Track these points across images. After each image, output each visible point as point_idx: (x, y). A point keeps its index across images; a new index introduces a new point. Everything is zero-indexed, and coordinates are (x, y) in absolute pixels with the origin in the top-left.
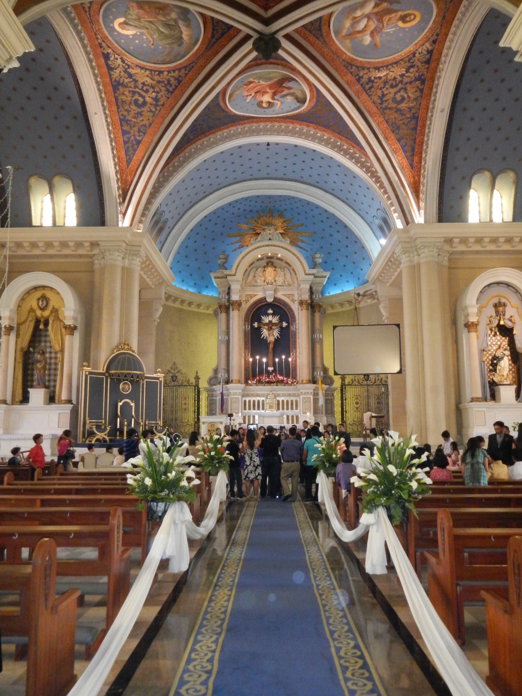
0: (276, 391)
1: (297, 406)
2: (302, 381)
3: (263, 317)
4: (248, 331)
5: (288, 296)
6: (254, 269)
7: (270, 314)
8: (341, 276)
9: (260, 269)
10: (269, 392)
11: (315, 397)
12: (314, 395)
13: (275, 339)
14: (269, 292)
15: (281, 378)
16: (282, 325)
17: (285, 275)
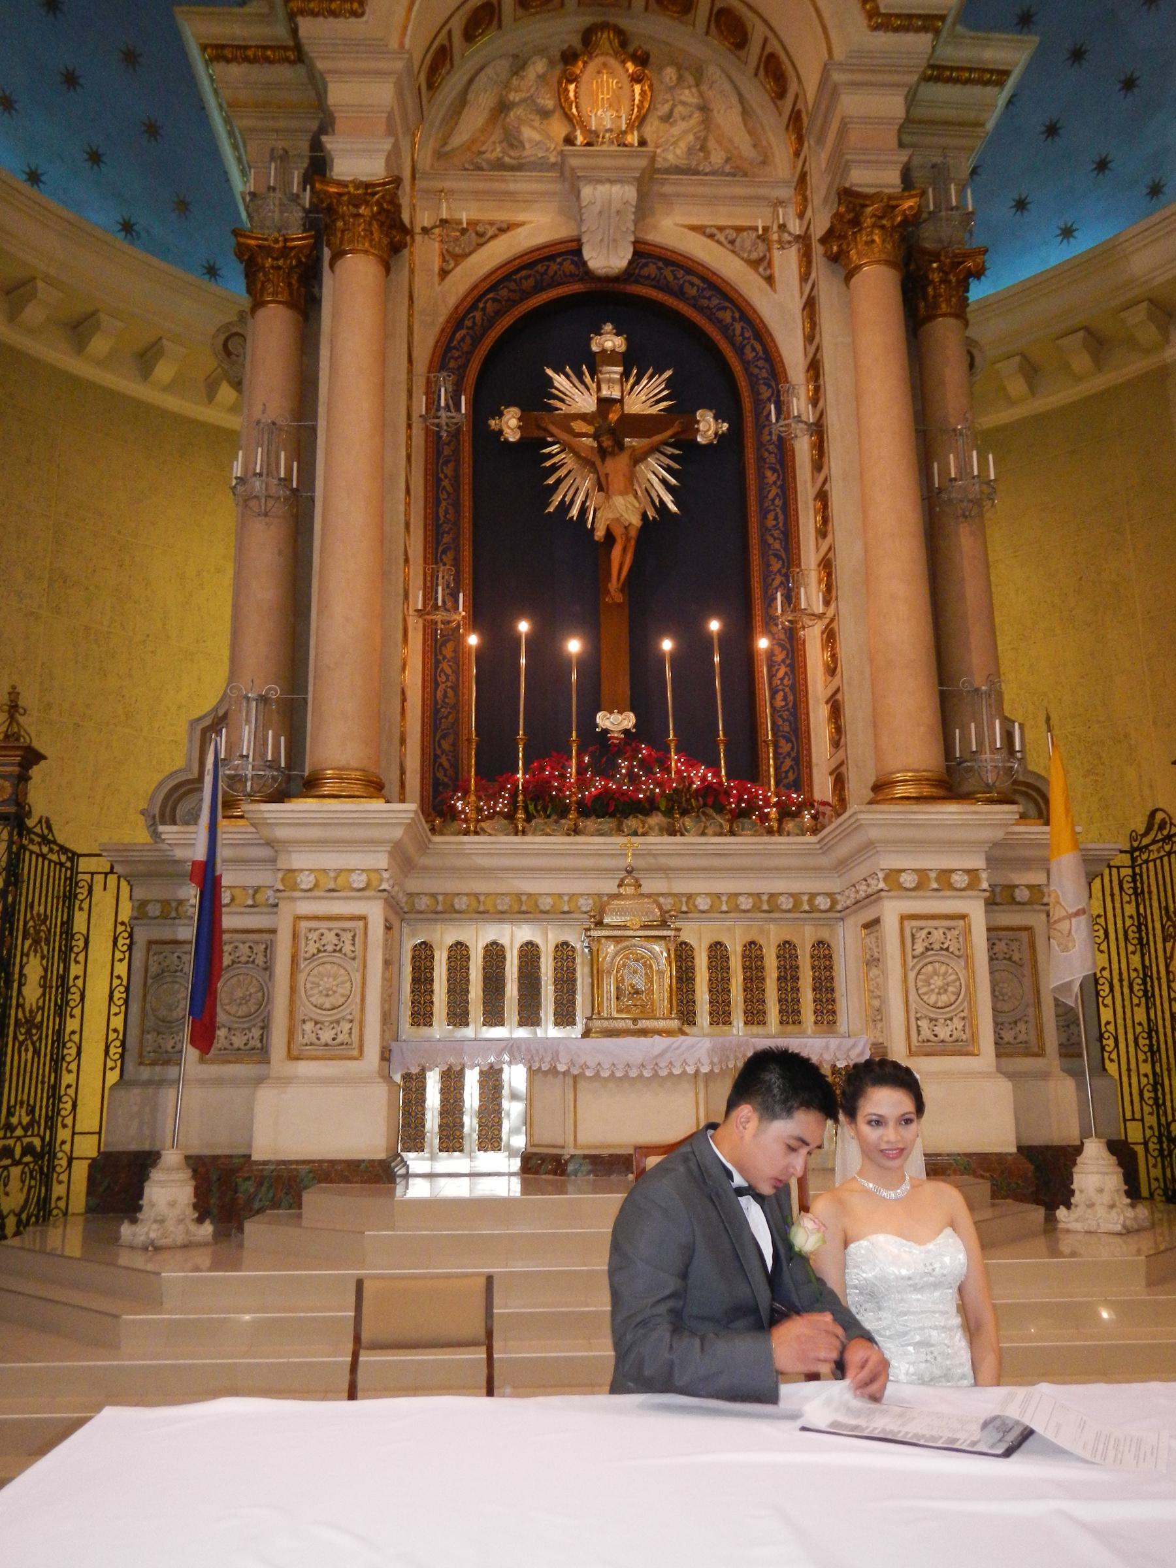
0: (666, 871)
1: (825, 987)
2: (881, 789)
3: (560, 381)
4: (456, 434)
5: (731, 237)
6: (502, 67)
7: (610, 357)
8: (1021, 205)
9: (539, 66)
10: (610, 886)
11: (1008, 918)
12: (991, 903)
13: (644, 516)
14: (602, 189)
15: (699, 775)
16: (691, 426)
17: (704, 109)
